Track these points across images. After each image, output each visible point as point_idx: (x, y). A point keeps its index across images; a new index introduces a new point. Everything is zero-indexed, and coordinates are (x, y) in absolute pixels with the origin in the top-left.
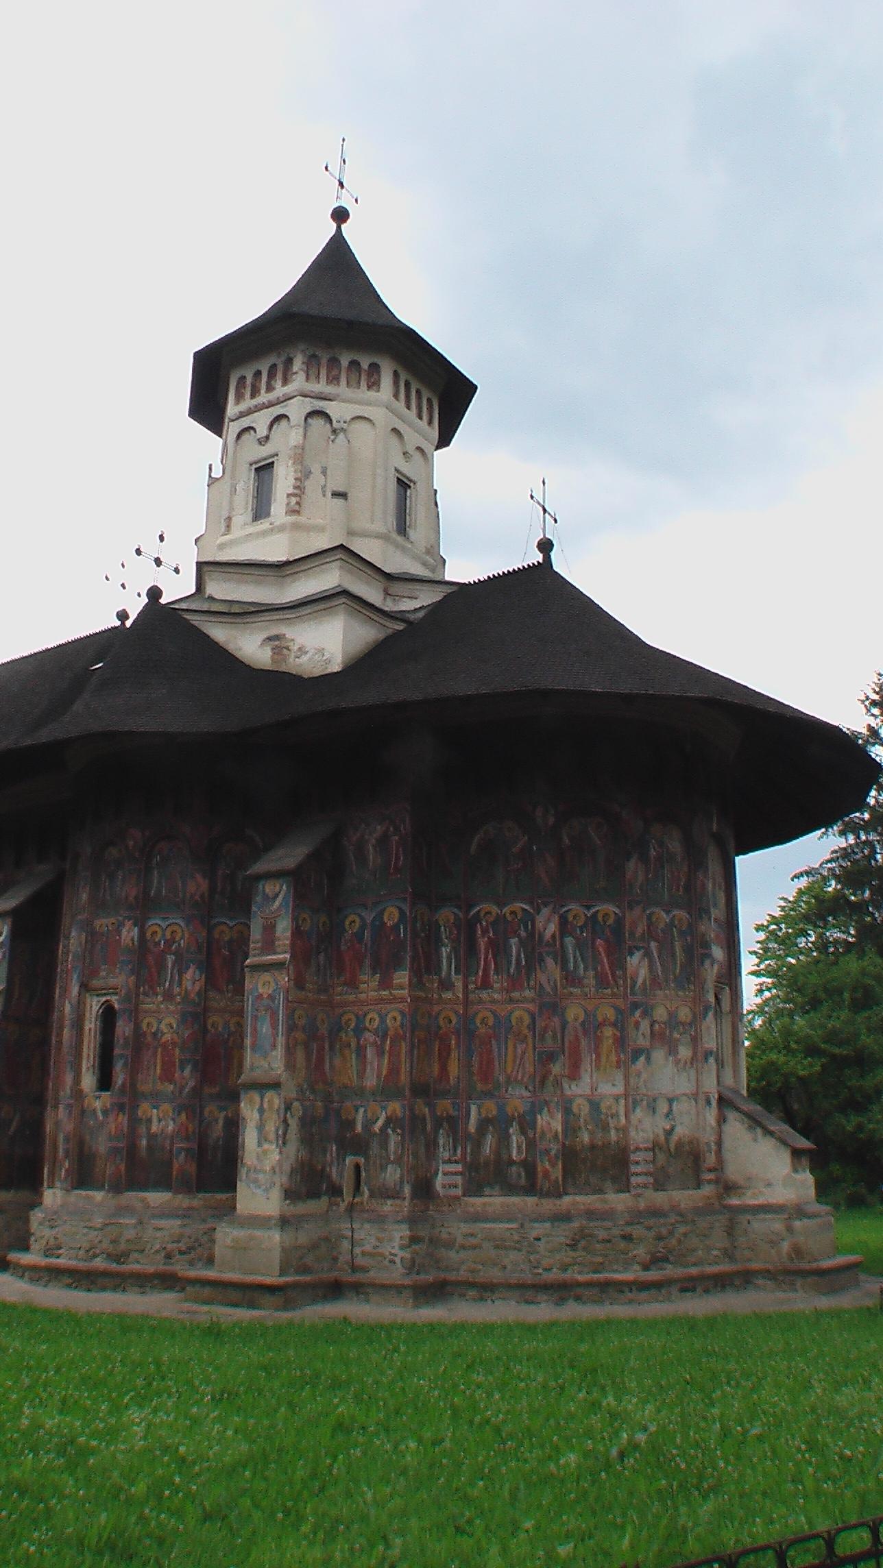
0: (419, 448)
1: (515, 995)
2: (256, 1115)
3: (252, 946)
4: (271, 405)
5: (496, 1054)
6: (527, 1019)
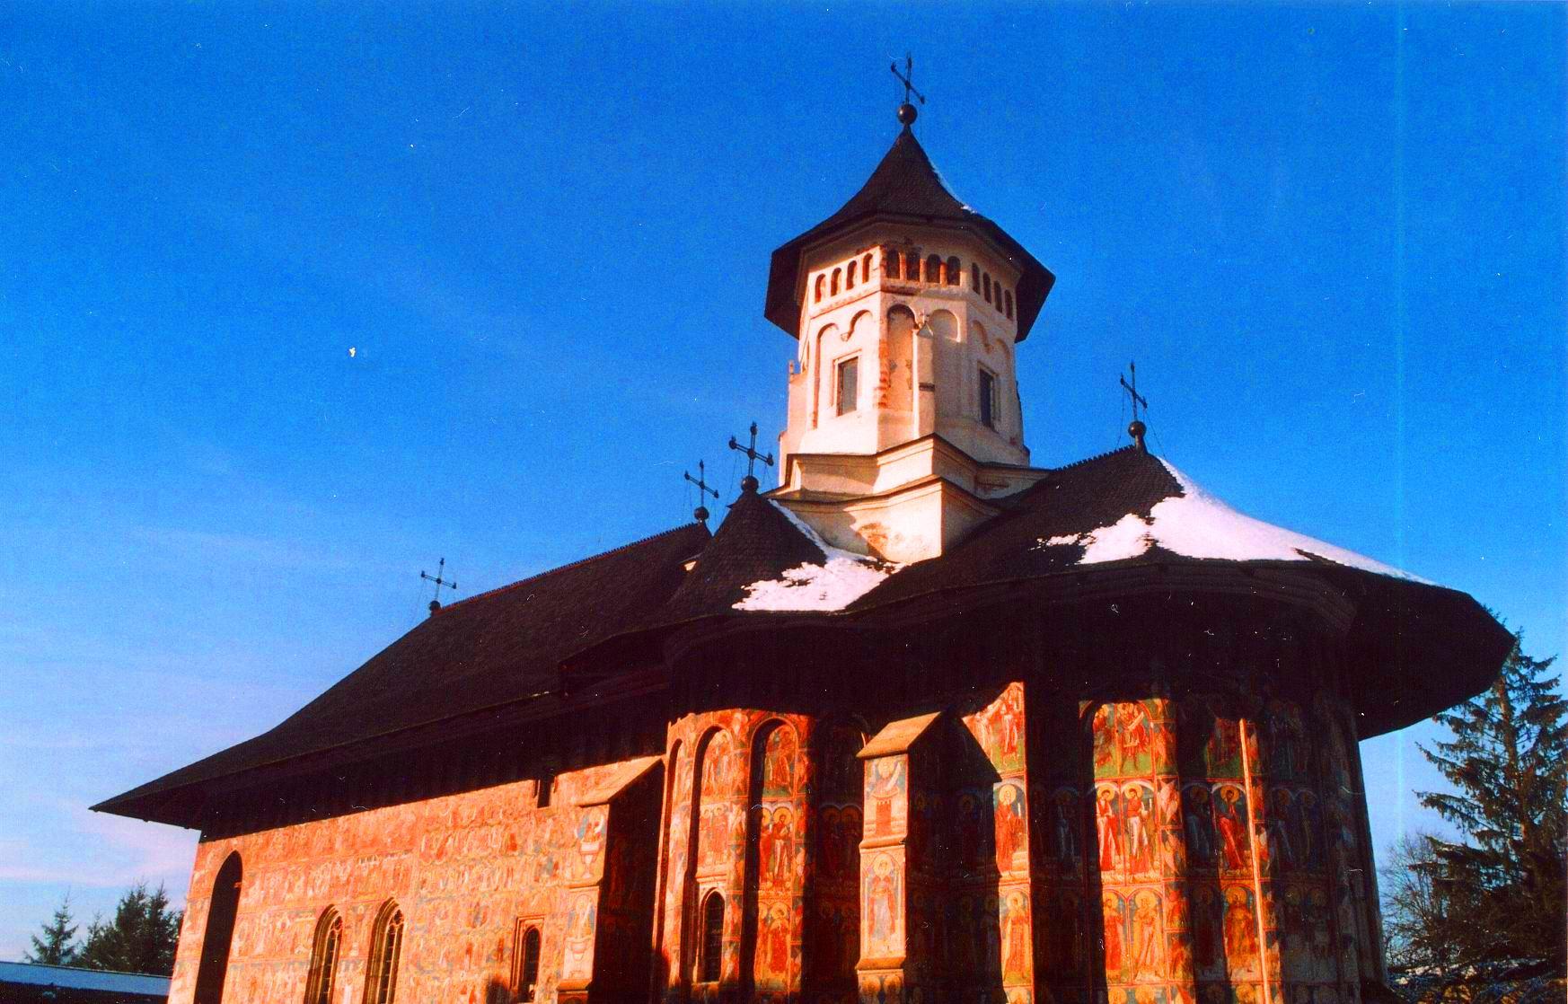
0: (1001, 341)
1: (1139, 876)
3: (865, 827)
4: (851, 302)
5: (1122, 937)
6: (1154, 902)
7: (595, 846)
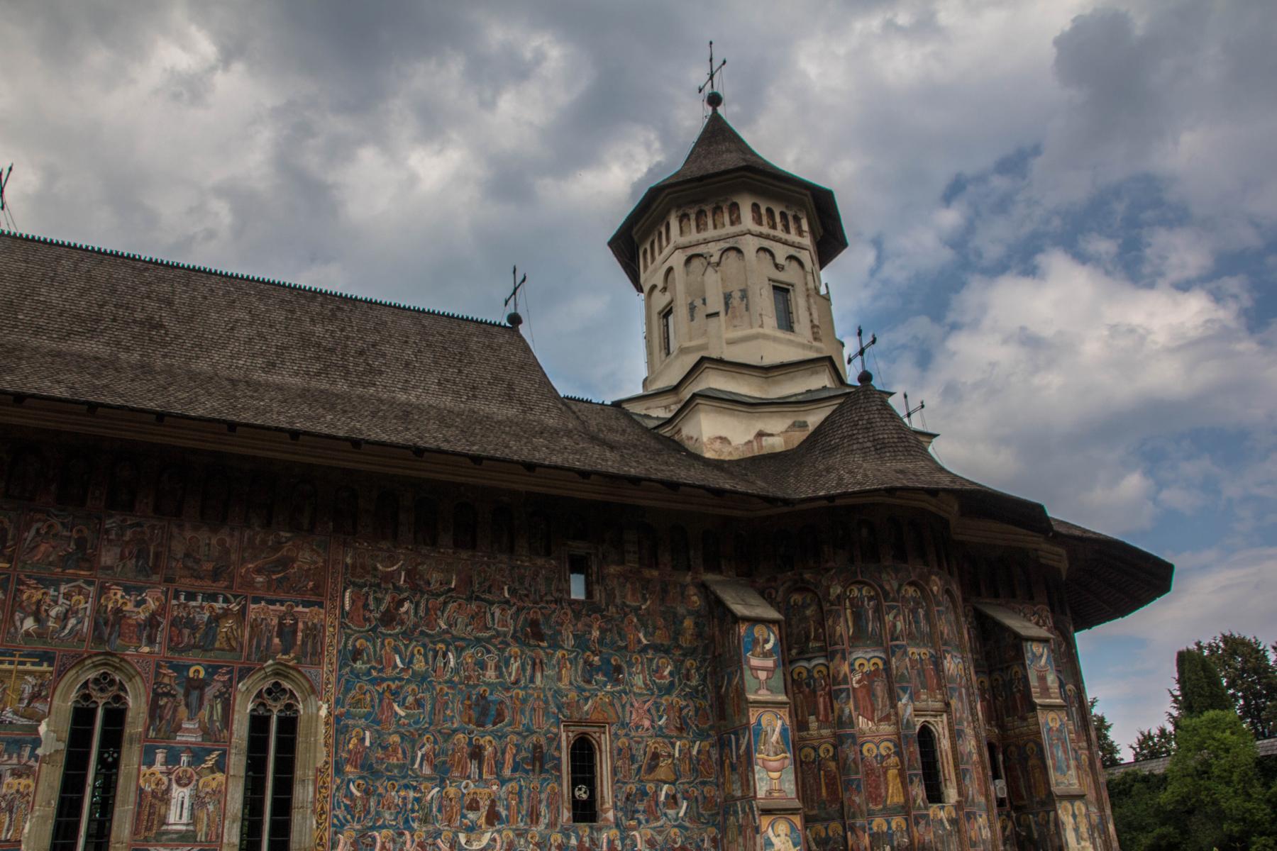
2: (1071, 820)
7: (769, 663)
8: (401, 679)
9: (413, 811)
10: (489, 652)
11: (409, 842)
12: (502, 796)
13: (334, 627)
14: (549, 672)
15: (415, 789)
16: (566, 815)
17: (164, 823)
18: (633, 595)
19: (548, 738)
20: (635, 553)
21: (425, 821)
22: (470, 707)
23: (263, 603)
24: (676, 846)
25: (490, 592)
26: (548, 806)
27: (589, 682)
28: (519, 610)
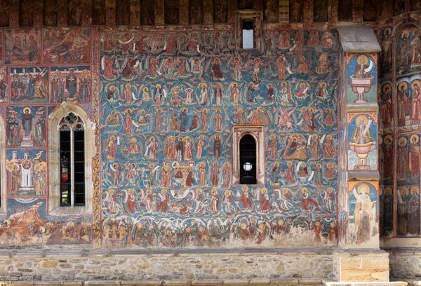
8: (135, 107)
9: (145, 179)
10: (187, 87)
11: (143, 195)
12: (196, 170)
13: (97, 80)
14: (224, 96)
15: (146, 167)
16: (235, 179)
17: (20, 187)
18: (284, 40)
19: (224, 136)
20: (286, 13)
21: (151, 184)
22: (176, 120)
23: (57, 70)
24: (305, 198)
25: (188, 50)
26: (224, 174)
27: (251, 101)
28: (207, 59)
